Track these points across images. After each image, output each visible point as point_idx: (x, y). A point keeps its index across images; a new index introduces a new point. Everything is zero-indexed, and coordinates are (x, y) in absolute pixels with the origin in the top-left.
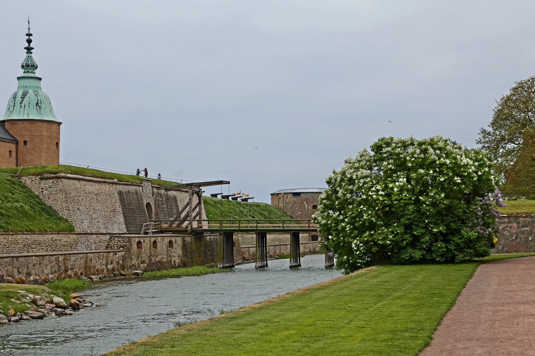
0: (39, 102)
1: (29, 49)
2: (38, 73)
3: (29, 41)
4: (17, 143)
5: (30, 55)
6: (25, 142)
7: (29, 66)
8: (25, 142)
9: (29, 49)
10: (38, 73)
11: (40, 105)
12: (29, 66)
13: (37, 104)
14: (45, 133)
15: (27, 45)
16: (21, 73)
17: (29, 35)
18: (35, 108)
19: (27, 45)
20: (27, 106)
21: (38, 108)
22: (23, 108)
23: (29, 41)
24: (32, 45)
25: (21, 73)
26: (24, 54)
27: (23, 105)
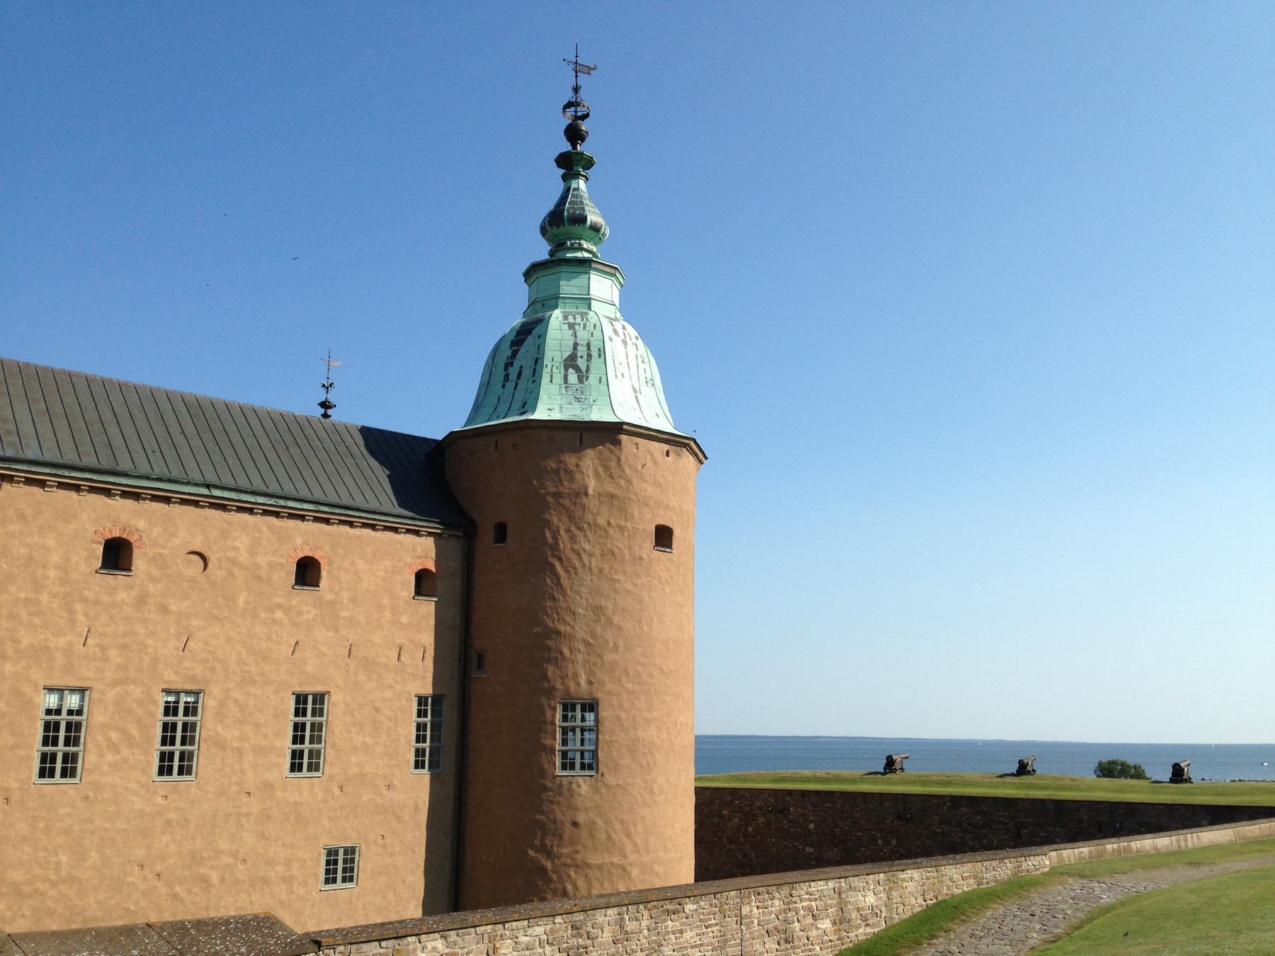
0: (582, 350)
3: (574, 134)
8: (501, 532)
11: (582, 363)
13: (570, 362)
15: (566, 146)
18: (558, 378)
19: (566, 146)
20: (527, 373)
21: (573, 378)
22: (510, 385)
23: (574, 134)
27: (513, 372)
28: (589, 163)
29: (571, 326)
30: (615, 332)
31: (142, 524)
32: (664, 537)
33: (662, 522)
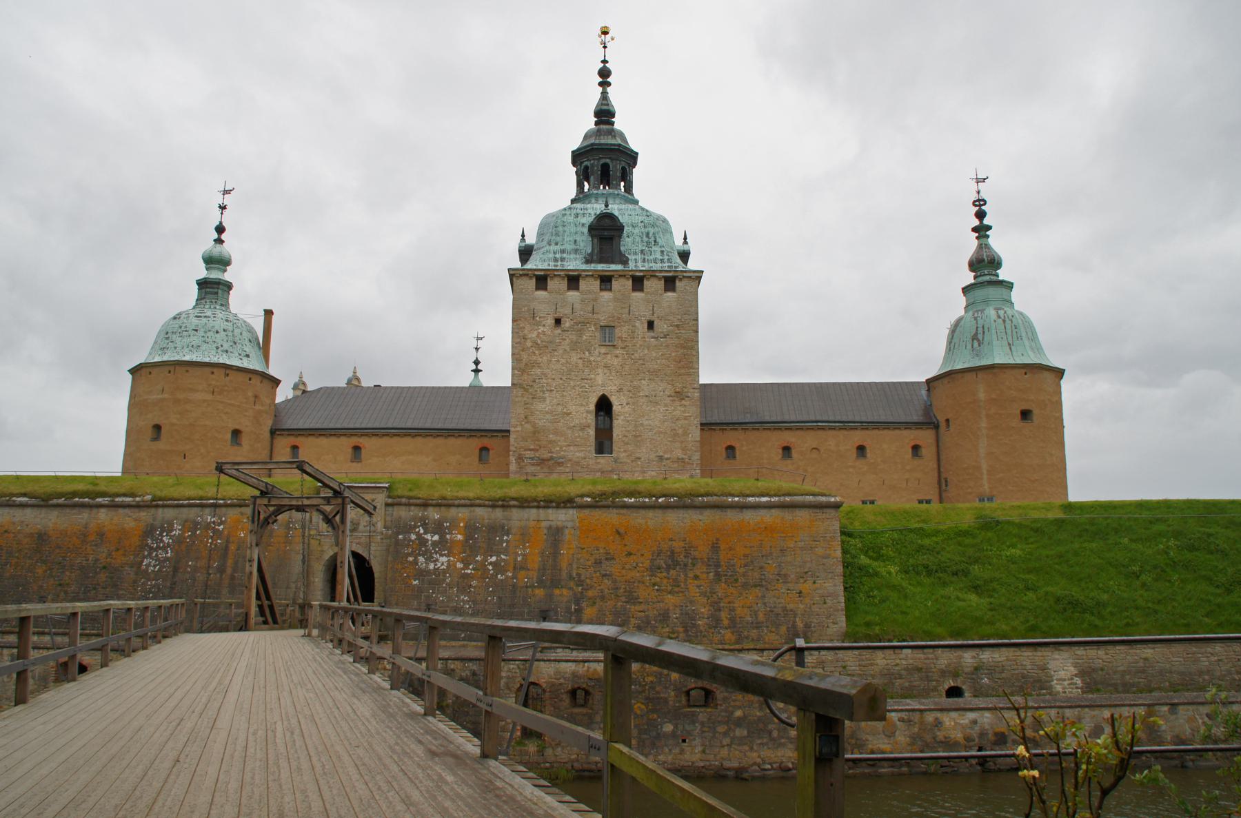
0: (980, 330)
1: (982, 231)
2: (1003, 274)
3: (981, 215)
4: (936, 427)
5: (983, 241)
6: (947, 421)
7: (985, 264)
8: (947, 421)
9: (982, 231)
10: (1003, 274)
11: (980, 337)
12: (985, 264)
13: (975, 337)
14: (982, 395)
15: (976, 222)
16: (969, 278)
17: (979, 203)
18: (969, 346)
19: (976, 222)
21: (976, 344)
23: (981, 215)
24: (986, 221)
25: (969, 278)
26: (972, 242)
28: (989, 228)
29: (976, 319)
30: (999, 317)
31: (793, 440)
32: (1025, 415)
33: (1024, 408)
